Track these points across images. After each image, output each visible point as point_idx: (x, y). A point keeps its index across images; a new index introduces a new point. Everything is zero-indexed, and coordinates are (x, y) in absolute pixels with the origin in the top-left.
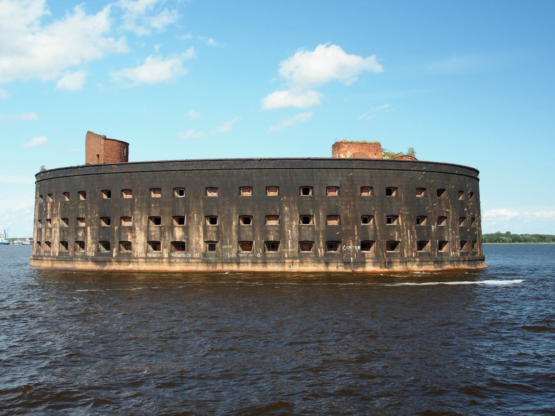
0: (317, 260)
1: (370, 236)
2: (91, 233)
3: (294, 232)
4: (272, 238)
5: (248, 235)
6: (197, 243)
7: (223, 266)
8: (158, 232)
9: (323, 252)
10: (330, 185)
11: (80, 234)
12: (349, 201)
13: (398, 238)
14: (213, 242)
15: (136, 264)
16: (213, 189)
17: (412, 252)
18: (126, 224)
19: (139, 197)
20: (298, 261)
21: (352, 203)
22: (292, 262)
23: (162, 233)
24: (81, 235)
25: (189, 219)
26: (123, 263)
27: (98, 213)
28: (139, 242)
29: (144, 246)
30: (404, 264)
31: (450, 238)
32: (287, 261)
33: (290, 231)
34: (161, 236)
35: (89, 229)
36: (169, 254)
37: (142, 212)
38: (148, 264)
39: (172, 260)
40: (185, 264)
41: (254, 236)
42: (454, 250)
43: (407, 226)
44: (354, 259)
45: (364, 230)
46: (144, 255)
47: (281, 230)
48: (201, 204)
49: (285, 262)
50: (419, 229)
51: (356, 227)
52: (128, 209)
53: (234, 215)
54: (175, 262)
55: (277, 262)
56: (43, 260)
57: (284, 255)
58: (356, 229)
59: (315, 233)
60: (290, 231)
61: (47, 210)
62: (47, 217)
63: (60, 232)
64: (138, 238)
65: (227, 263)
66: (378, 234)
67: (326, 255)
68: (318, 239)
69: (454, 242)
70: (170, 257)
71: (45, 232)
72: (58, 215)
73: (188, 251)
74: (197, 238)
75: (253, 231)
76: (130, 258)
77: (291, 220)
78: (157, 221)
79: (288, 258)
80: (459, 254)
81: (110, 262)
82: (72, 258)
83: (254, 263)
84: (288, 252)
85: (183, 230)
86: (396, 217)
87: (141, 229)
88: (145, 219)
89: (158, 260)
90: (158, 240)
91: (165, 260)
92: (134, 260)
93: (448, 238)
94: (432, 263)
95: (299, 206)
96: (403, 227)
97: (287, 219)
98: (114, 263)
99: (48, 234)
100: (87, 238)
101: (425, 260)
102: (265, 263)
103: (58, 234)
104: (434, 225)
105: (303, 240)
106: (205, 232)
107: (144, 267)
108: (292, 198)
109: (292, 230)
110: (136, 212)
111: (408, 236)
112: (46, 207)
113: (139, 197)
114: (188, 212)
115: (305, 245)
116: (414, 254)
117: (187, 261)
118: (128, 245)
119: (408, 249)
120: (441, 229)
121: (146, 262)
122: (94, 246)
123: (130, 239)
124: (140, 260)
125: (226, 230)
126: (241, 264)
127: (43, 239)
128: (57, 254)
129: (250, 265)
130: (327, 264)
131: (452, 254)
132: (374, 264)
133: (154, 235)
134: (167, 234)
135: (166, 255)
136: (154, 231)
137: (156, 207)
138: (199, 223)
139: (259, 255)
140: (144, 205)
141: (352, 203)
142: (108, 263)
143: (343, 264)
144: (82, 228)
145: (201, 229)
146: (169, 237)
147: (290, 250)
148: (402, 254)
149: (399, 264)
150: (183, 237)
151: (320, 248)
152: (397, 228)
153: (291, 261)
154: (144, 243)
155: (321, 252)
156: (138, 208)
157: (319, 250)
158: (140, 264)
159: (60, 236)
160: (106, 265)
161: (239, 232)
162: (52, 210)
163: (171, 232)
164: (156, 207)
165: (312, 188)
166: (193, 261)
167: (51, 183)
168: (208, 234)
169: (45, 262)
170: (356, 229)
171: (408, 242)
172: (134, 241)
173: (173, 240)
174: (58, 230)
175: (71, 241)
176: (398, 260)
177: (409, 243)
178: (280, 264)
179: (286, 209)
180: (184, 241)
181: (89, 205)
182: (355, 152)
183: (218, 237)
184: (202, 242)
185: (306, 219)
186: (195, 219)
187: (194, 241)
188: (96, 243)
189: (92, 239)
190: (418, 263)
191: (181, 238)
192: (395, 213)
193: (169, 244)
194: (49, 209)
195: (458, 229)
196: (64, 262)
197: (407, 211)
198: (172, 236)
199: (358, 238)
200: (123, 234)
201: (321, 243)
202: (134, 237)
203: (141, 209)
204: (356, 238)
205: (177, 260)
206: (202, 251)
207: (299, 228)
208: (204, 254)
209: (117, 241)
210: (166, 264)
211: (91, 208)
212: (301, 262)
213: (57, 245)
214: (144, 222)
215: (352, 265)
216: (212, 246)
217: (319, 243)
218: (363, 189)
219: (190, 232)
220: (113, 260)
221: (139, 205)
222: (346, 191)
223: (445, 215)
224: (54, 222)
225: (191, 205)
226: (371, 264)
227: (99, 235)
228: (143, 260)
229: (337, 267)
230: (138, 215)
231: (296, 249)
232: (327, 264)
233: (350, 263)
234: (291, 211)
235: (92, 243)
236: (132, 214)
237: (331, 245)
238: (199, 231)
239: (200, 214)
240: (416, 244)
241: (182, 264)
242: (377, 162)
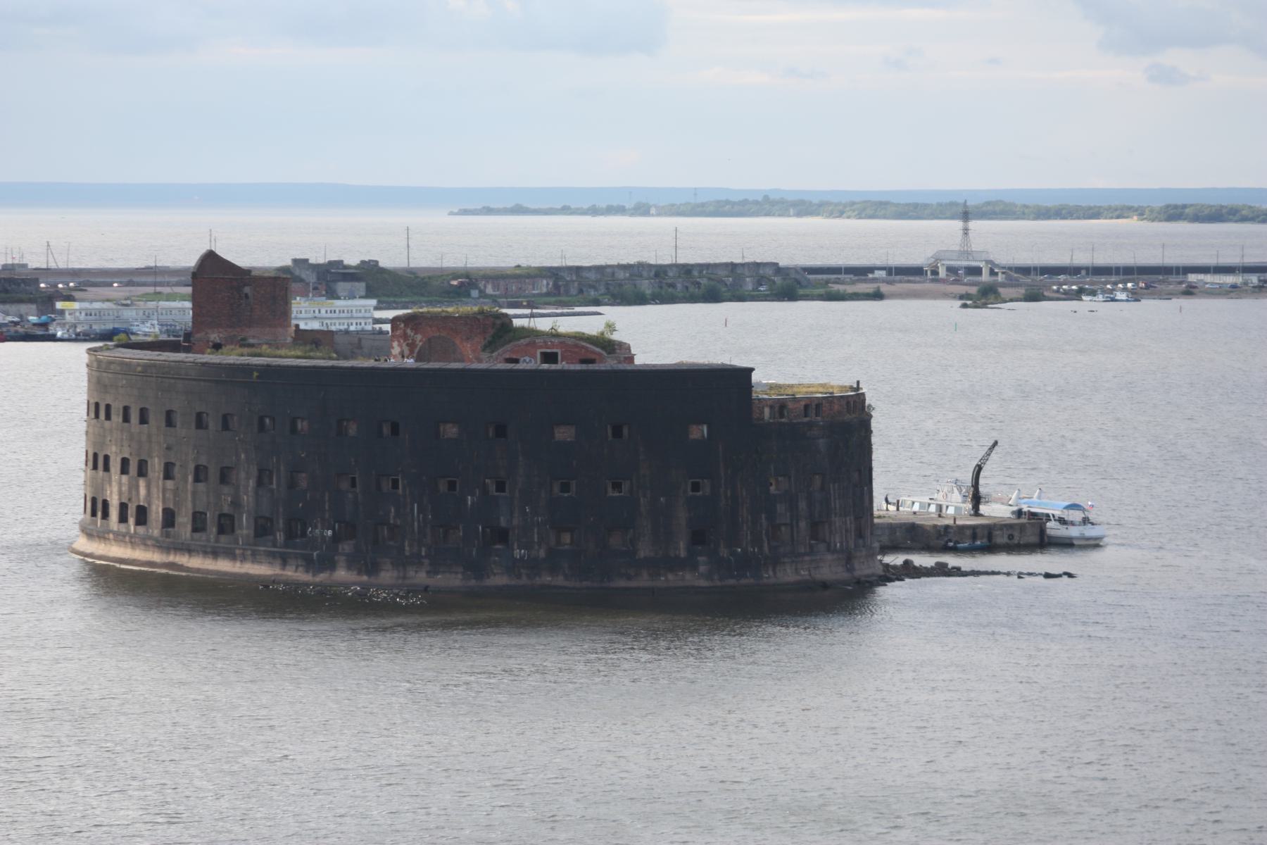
0: (272, 555)
4: (226, 510)
31: (515, 522)
77: (248, 478)
80: (542, 554)
94: (461, 569)
104: (473, 495)
116: (423, 549)
147: (245, 532)
155: (280, 537)
166: (149, 542)
184: (160, 510)
201: (281, 521)
204: (327, 516)
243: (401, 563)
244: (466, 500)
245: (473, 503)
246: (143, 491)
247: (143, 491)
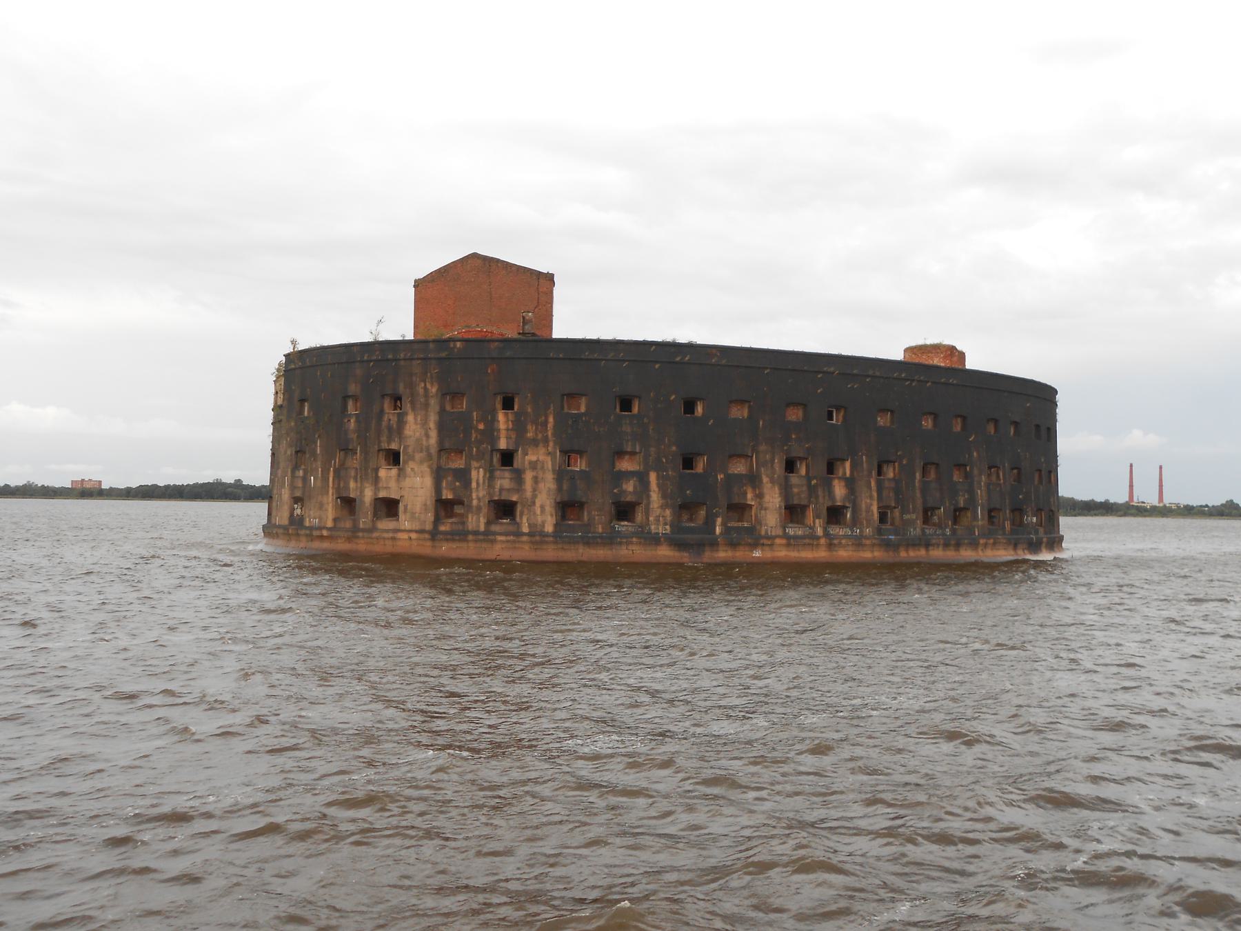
2: (658, 485)
6: (868, 510)
7: (907, 551)
8: (804, 488)
11: (629, 486)
14: (888, 507)
15: (767, 548)
18: (739, 468)
23: (812, 490)
24: (631, 489)
26: (741, 548)
28: (770, 505)
32: (982, 541)
35: (653, 477)
36: (825, 530)
39: (836, 542)
46: (780, 532)
64: (767, 498)
65: (914, 545)
70: (826, 534)
73: (855, 522)
76: (754, 537)
81: (714, 544)
83: (946, 545)
85: (846, 486)
87: (772, 481)
90: (804, 502)
91: (823, 541)
92: (766, 542)
97: (976, 472)
98: (721, 548)
100: (649, 497)
102: (958, 546)
103: (549, 482)
107: (782, 553)
110: (763, 448)
117: (858, 543)
121: (788, 545)
122: (668, 512)
124: (778, 541)
128: (549, 528)
133: (798, 494)
134: (820, 493)
135: (820, 532)
139: (948, 532)
144: (628, 475)
145: (873, 484)
159: (560, 489)
161: (924, 491)
166: (868, 542)
168: (885, 493)
172: (760, 504)
173: (830, 504)
174: (550, 476)
184: (875, 509)
187: (863, 506)
189: (664, 496)
193: (825, 512)
202: (760, 496)
205: (844, 541)
208: (879, 531)
214: (779, 467)
216: (883, 518)
228: (784, 541)
235: (663, 507)
238: (870, 487)
246: (839, 490)
247: (839, 490)
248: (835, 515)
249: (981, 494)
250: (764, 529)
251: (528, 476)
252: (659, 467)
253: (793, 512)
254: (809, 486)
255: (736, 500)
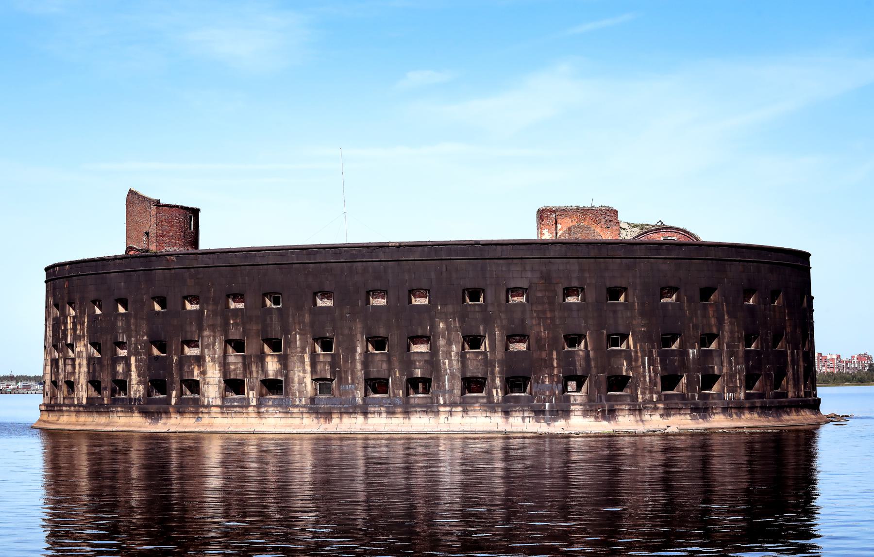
1: (578, 367)
2: (136, 367)
3: (455, 363)
4: (418, 373)
5: (380, 368)
6: (301, 382)
8: (240, 365)
9: (500, 394)
10: (512, 285)
12: (544, 312)
13: (627, 370)
14: (326, 379)
16: (326, 295)
17: (651, 393)
18: (189, 351)
19: (210, 308)
20: (460, 409)
21: (549, 315)
22: (451, 412)
23: (246, 367)
24: (121, 370)
25: (288, 343)
26: (187, 415)
27: (146, 334)
29: (219, 387)
30: (637, 413)
31: (725, 370)
32: (442, 409)
33: (447, 361)
34: (245, 370)
35: (133, 359)
37: (214, 332)
38: (226, 415)
39: (263, 410)
40: (282, 415)
41: (390, 370)
42: (732, 390)
43: (643, 351)
44: (551, 406)
45: (567, 360)
46: (219, 402)
47: (432, 361)
48: (307, 318)
49: (438, 412)
50: (664, 356)
51: (555, 353)
52: (194, 328)
53: (359, 336)
54: (267, 412)
55: (426, 412)
56: (62, 411)
57: (438, 400)
58: (555, 356)
59: (488, 363)
60: (447, 361)
61: (66, 329)
62: (66, 340)
63: (88, 365)
64: (209, 375)
66: (593, 364)
67: (506, 399)
68: (493, 373)
69: (732, 376)
70: (259, 405)
71: (65, 365)
72: (84, 337)
74: (301, 374)
75: (389, 361)
77: (450, 343)
78: (239, 346)
79: (445, 405)
80: (742, 396)
81: (167, 413)
82: (108, 408)
83: (391, 413)
84: (444, 396)
85: (279, 361)
86: (625, 337)
87: (213, 360)
88: (220, 343)
89: (240, 410)
90: (240, 377)
91: (251, 409)
92: (204, 410)
93: (721, 370)
94: (689, 412)
95: (462, 321)
96: (636, 352)
97: (442, 342)
99: (69, 368)
100: (130, 375)
101: (674, 406)
102: (407, 413)
103: (84, 369)
104: (693, 348)
105: (469, 375)
106: (313, 365)
108: (450, 308)
109: (450, 360)
110: (206, 333)
111: (644, 367)
112: (66, 324)
113: (210, 308)
114: (286, 331)
115: (472, 384)
116: (655, 396)
118: (194, 386)
119: (645, 389)
120: (706, 356)
121: (222, 413)
122: (141, 387)
123: (196, 375)
124: (213, 409)
125: (346, 361)
126: (369, 416)
127: (61, 376)
128: (84, 402)
129: (384, 415)
130: (507, 413)
131: (727, 396)
132: (585, 413)
133: (235, 370)
134: (254, 369)
136: (234, 363)
137: (236, 324)
138: (303, 350)
140: (219, 320)
141: (549, 315)
142: (163, 415)
143: (532, 415)
144: (123, 358)
146: (257, 372)
148: (634, 398)
149: (627, 412)
150: (279, 372)
151: (496, 388)
152: (627, 354)
153: (448, 409)
154: (219, 382)
155: (498, 395)
156: (209, 326)
157: (494, 391)
158: (213, 415)
160: (161, 418)
161: (366, 364)
162: (74, 329)
163: (260, 365)
164: (236, 324)
165: (483, 290)
167: (70, 284)
168: (319, 368)
169: (66, 414)
170: (555, 356)
171: (644, 376)
172: (204, 379)
173: (263, 378)
174: (85, 362)
175: (106, 379)
176: (627, 407)
177: (647, 378)
178: (431, 415)
179: (441, 325)
180: (280, 378)
181: (132, 321)
182: (571, 224)
183: (333, 373)
184: (308, 380)
185: (474, 341)
186: (298, 343)
187: (296, 379)
188: (144, 383)
189: (139, 376)
190: (662, 412)
191: (276, 375)
192: (622, 330)
193: (258, 384)
194: (69, 327)
195: (741, 354)
196: (95, 414)
197: (643, 326)
198: (262, 371)
199: (559, 372)
200: (186, 368)
201: (498, 380)
202: (204, 373)
203: (213, 328)
204: (555, 372)
206: (310, 395)
207: (463, 356)
208: (312, 400)
209: (177, 378)
210: (254, 415)
211: (136, 327)
212: (465, 411)
213: (84, 387)
215: (548, 416)
217: (494, 380)
218: (569, 291)
219: (290, 364)
220: (171, 410)
221: (211, 322)
222: (539, 294)
223: (715, 331)
224: (78, 349)
225: (291, 320)
226: (579, 413)
227: (149, 369)
228: (218, 410)
229: (523, 418)
230: (209, 337)
231: (457, 391)
232: (507, 413)
233: (543, 412)
234: (448, 328)
235: (139, 383)
236: (201, 336)
237: (515, 382)
238: (303, 362)
239: (305, 335)
240: (659, 380)
241: (279, 415)
242: (591, 246)
243: (637, 409)
244: (688, 355)
245: (694, 355)
246: (272, 366)
247: (272, 366)
248: (273, 386)
249: (450, 363)
250: (206, 400)
251: (77, 363)
252: (137, 354)
253: (234, 385)
254: (244, 364)
255: (186, 378)
